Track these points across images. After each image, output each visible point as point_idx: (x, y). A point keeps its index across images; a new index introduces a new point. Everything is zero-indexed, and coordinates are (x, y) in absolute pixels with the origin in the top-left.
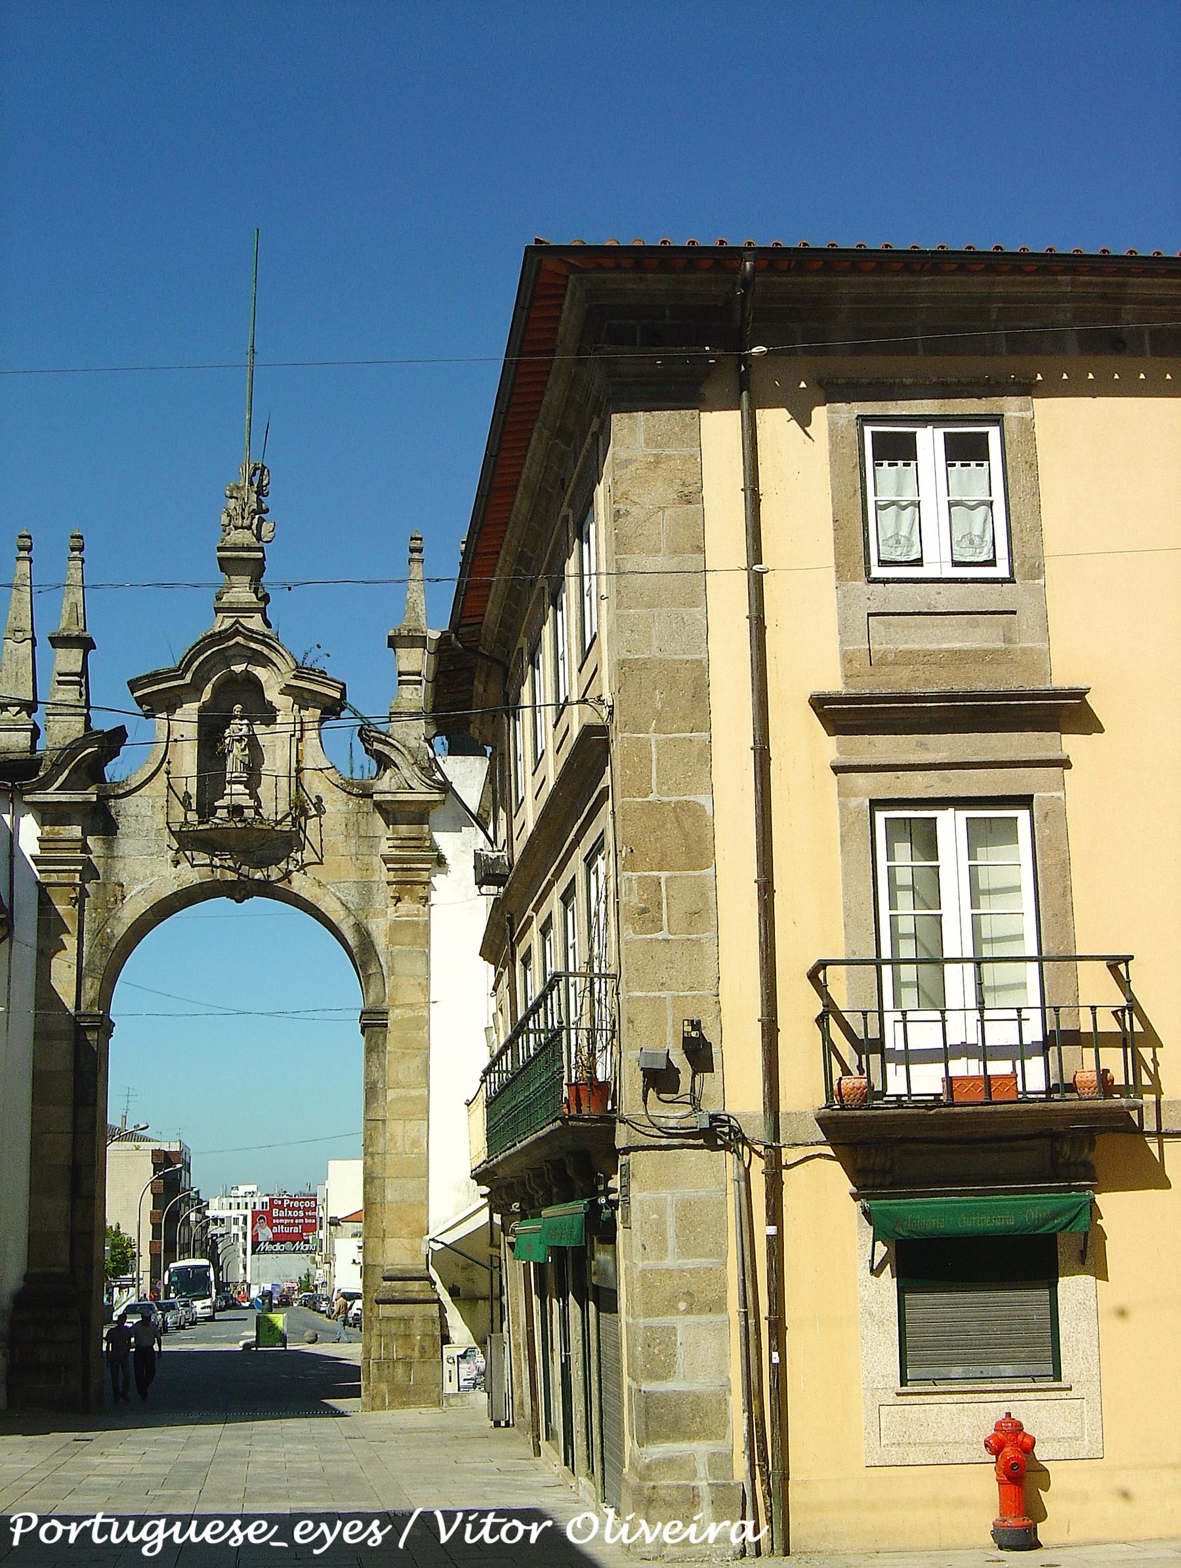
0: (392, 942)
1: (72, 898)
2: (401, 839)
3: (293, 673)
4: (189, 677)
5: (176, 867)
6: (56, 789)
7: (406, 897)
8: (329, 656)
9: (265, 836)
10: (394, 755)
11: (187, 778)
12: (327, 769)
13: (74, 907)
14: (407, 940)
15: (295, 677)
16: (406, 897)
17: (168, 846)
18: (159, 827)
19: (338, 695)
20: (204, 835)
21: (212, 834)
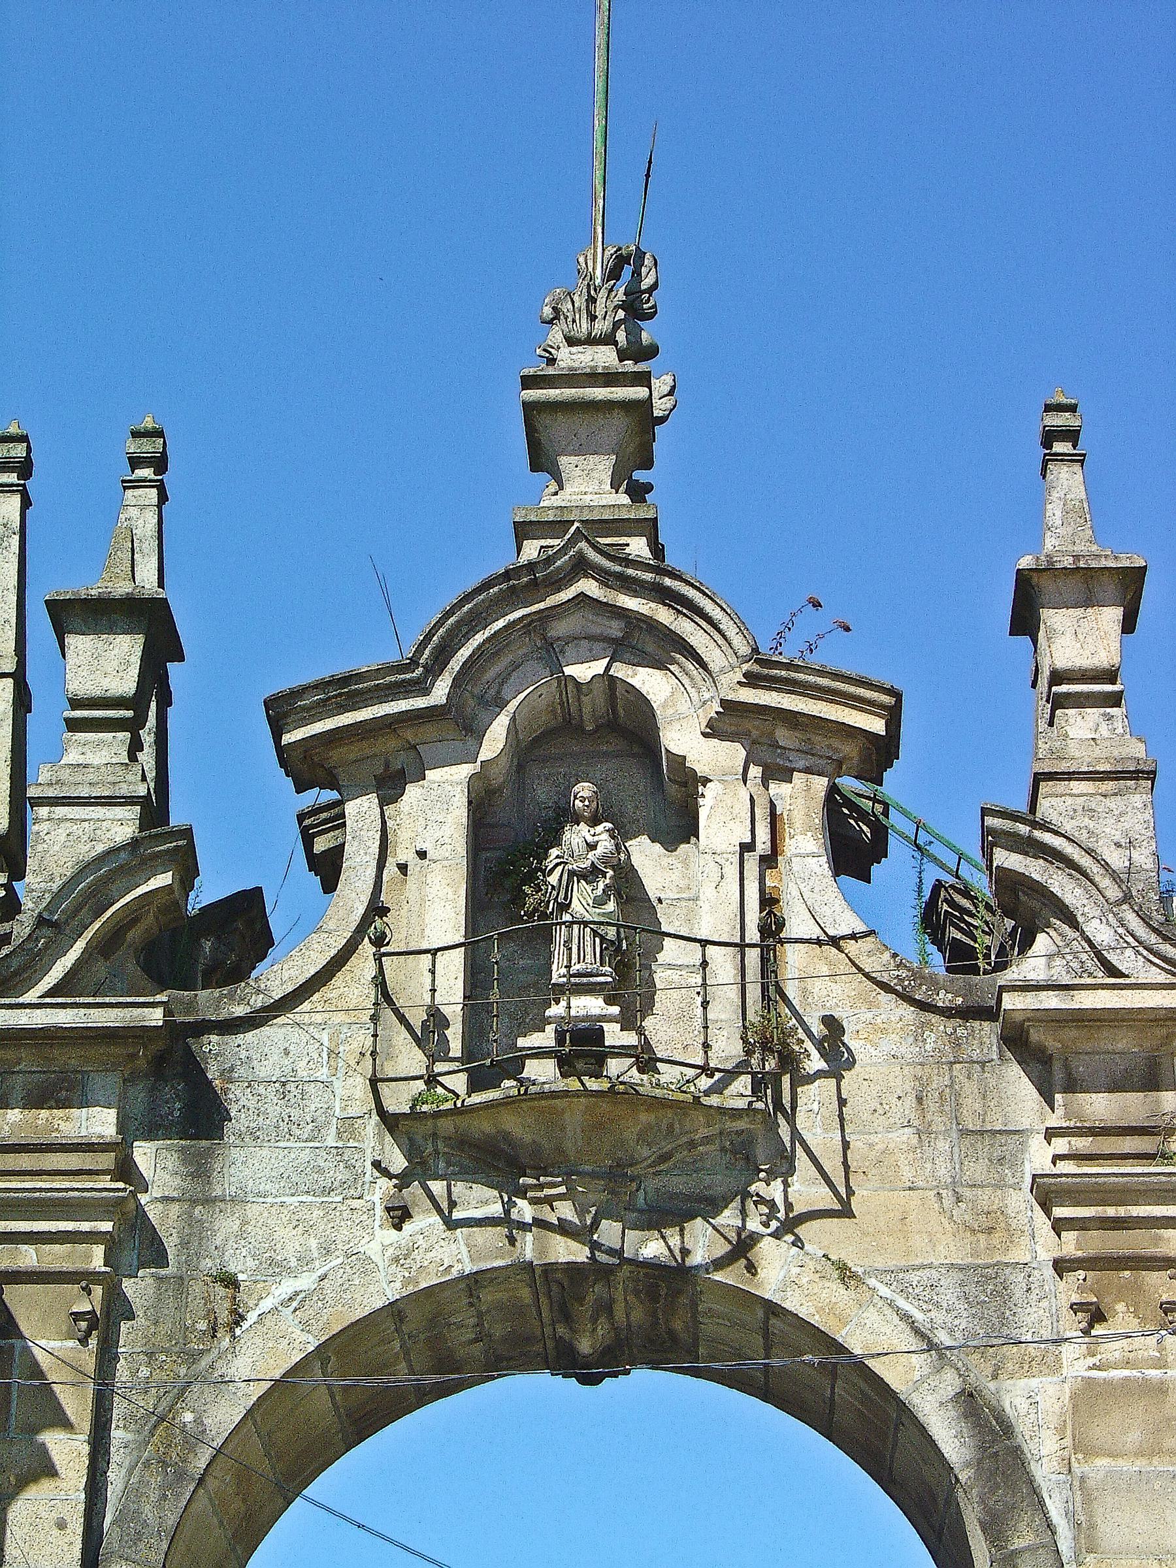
0: (1083, 1447)
1: (77, 1317)
2: (1093, 1132)
3: (745, 667)
4: (440, 691)
5: (400, 1229)
6: (50, 993)
7: (1120, 1307)
8: (847, 629)
9: (671, 1127)
10: (1060, 884)
11: (434, 952)
12: (853, 937)
13: (84, 1341)
14: (1133, 1437)
15: (751, 680)
16: (1120, 1307)
17: (376, 1165)
18: (351, 1112)
19: (877, 726)
20: (484, 1126)
21: (513, 1124)
